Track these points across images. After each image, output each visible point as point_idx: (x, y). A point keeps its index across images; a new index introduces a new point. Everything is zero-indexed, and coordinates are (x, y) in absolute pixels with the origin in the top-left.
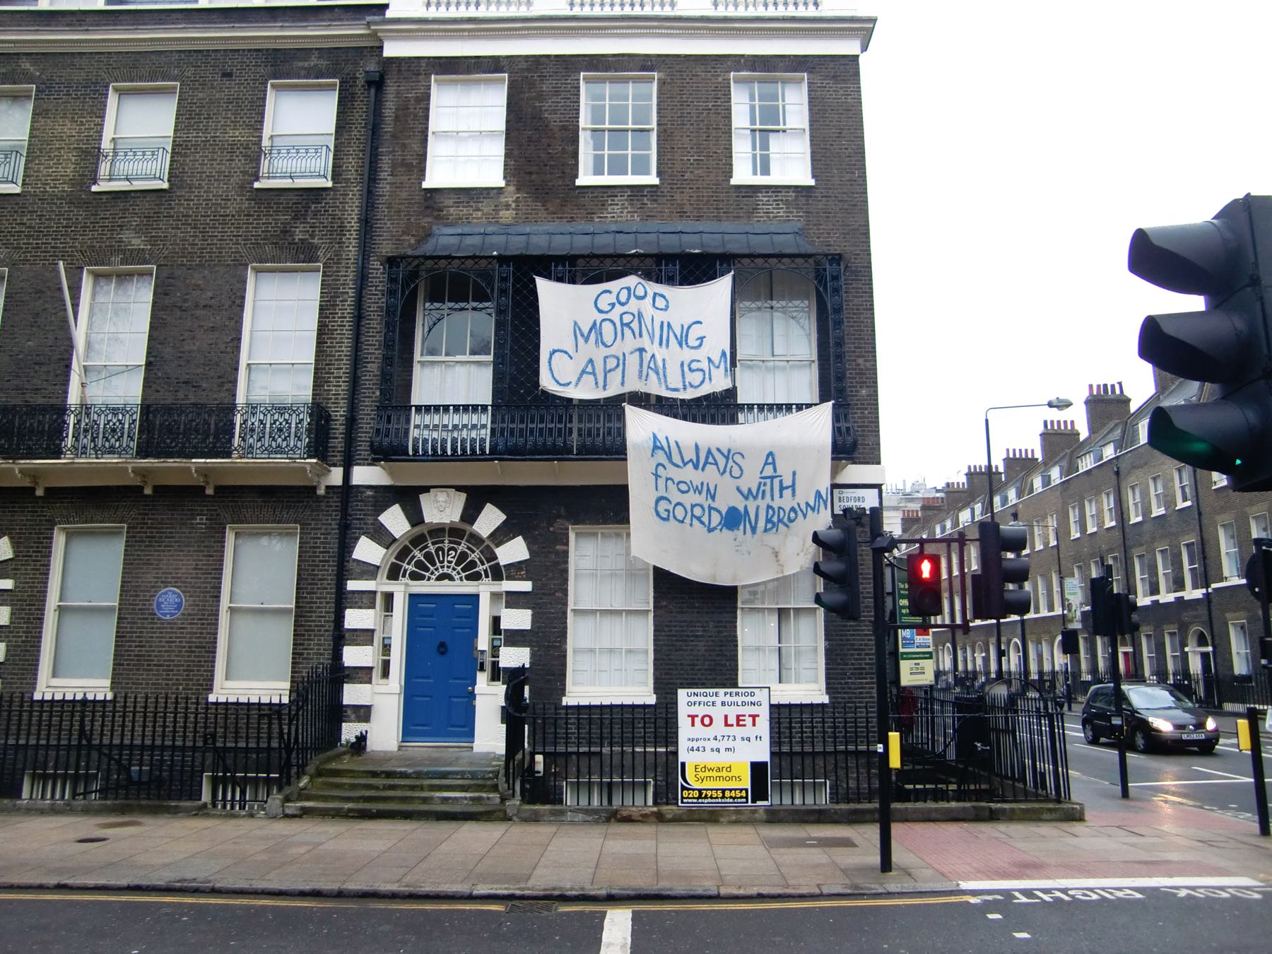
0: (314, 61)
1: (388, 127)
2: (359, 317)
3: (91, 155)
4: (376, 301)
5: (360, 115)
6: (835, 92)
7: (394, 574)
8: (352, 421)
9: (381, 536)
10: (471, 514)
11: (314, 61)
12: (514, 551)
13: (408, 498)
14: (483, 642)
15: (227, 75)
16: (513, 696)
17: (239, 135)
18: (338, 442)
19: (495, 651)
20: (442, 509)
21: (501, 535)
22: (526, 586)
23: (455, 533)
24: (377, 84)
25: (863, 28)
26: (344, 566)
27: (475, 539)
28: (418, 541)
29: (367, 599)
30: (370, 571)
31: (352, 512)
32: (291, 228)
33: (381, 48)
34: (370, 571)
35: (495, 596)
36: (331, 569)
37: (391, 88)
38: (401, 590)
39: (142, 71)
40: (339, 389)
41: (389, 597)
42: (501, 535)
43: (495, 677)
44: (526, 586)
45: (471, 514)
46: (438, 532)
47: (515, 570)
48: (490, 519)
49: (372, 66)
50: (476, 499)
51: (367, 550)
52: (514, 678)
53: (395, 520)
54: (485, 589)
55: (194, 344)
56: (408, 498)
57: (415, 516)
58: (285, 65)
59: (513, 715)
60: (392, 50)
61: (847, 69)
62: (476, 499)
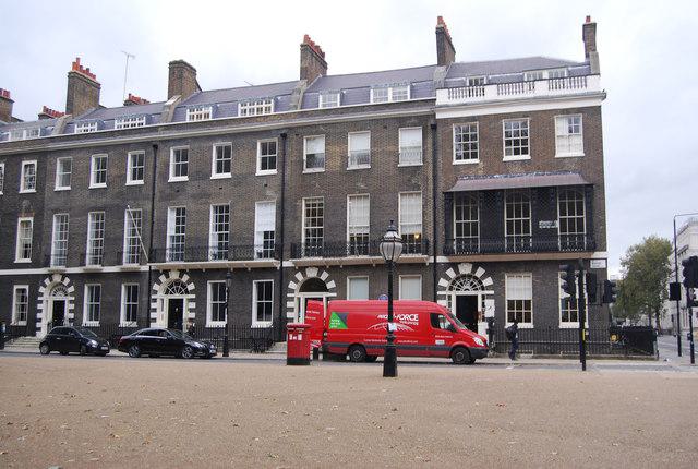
0: (413, 120)
1: (440, 143)
2: (435, 208)
3: (345, 158)
4: (440, 203)
5: (430, 140)
6: (590, 120)
7: (451, 289)
8: (435, 242)
9: (447, 278)
10: (474, 270)
11: (413, 120)
12: (488, 282)
13: (455, 266)
14: (480, 309)
15: (386, 127)
16: (490, 325)
17: (391, 148)
18: (431, 249)
19: (483, 312)
20: (465, 269)
21: (484, 277)
22: (492, 292)
23: (469, 276)
24: (434, 127)
25: (603, 96)
26: (436, 287)
27: (476, 278)
28: (457, 279)
29: (443, 297)
30: (444, 289)
31: (436, 271)
32: (409, 179)
33: (435, 115)
34: (444, 289)
35: (483, 297)
36: (432, 288)
37: (439, 129)
38: (454, 294)
39: (358, 126)
40: (430, 231)
41: (450, 296)
42: (484, 277)
43: (484, 320)
44: (492, 292)
45: (474, 270)
46: (464, 276)
47: (489, 288)
48: (480, 272)
49: (432, 122)
50: (476, 266)
51: (443, 282)
52: (490, 320)
53: (451, 273)
54: (479, 294)
55: (383, 216)
56: (455, 266)
57: (457, 271)
58: (403, 122)
59: (489, 332)
60: (438, 116)
61: (596, 112)
62: (476, 266)
